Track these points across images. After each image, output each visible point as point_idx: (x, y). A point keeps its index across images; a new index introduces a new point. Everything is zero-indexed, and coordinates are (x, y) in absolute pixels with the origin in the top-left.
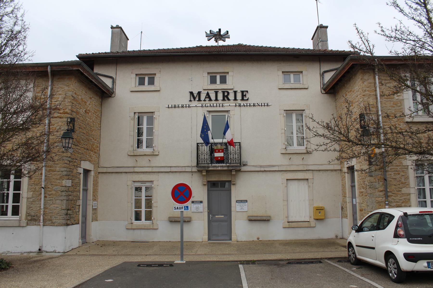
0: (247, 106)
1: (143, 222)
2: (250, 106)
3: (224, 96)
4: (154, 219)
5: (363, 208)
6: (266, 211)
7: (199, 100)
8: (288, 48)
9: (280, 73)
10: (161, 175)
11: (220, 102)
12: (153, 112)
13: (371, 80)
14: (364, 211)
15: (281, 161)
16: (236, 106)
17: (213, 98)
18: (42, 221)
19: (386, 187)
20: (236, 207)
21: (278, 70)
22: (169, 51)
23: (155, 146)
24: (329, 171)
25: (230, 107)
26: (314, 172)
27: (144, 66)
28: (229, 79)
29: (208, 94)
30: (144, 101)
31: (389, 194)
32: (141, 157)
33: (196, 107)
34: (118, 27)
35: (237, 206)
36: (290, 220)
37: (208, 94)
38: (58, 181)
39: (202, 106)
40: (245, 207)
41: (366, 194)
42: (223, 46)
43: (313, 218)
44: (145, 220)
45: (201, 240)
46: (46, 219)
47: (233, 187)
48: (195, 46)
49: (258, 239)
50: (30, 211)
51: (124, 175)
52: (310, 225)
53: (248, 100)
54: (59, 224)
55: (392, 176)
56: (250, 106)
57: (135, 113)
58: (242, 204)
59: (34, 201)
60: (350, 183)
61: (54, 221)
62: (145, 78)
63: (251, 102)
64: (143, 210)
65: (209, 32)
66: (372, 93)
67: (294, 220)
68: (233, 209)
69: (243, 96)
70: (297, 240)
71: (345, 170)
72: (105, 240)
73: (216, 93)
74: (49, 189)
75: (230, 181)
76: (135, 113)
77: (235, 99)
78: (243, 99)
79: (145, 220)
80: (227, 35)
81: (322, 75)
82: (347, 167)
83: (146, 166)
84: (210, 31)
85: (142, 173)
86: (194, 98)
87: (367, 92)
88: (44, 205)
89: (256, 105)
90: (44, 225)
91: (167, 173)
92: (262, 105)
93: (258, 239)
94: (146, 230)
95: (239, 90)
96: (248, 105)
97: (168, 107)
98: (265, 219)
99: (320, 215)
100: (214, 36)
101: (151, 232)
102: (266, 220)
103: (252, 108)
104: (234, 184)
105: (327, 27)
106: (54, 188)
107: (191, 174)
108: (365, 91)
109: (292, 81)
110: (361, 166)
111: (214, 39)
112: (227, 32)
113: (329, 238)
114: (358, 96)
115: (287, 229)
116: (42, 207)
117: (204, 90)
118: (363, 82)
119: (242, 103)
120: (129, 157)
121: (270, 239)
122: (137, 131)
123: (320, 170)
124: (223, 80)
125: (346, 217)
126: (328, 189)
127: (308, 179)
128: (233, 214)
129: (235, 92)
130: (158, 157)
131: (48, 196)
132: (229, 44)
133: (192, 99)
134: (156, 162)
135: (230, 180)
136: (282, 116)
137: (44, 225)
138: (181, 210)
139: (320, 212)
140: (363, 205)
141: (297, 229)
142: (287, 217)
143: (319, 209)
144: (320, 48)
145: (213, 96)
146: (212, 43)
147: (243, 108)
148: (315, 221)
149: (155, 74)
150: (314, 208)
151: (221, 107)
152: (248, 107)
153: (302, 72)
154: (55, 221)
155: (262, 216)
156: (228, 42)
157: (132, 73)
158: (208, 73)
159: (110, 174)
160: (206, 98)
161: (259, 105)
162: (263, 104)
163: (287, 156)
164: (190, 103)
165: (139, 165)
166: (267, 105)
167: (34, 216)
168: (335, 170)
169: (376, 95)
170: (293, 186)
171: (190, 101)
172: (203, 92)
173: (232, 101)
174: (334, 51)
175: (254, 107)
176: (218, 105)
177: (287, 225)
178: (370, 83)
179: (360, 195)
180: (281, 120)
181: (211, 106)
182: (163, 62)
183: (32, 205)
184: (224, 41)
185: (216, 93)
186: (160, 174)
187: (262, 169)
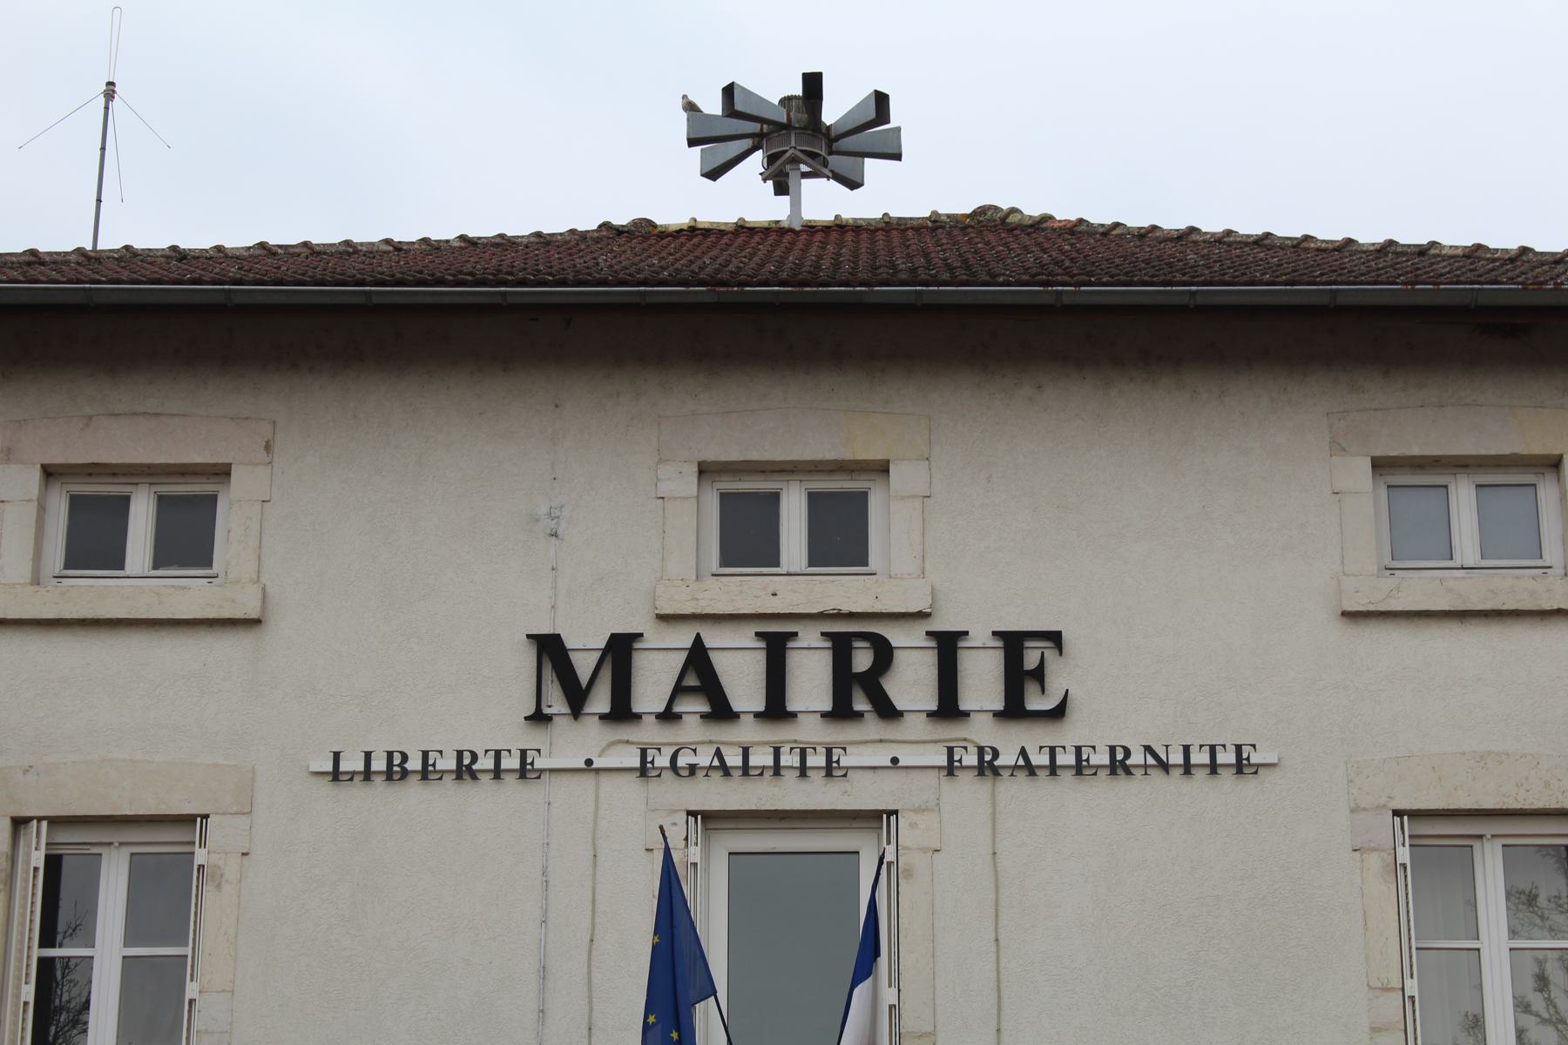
0: (1053, 769)
2: (1079, 768)
3: (843, 680)
7: (622, 712)
8: (1422, 251)
11: (810, 730)
12: (187, 820)
16: (951, 769)
17: (745, 690)
21: (1337, 447)
22: (353, 267)
25: (894, 779)
28: (891, 522)
29: (698, 658)
33: (588, 781)
37: (698, 658)
39: (643, 771)
42: (840, 228)
48: (588, 223)
56: (1079, 768)
57: (19, 823)
62: (125, 501)
63: (1087, 730)
65: (712, 105)
69: (1019, 678)
73: (776, 649)
76: (19, 823)
77: (948, 708)
78: (1013, 710)
80: (874, 131)
84: (729, 91)
86: (577, 698)
89: (1137, 758)
92: (1187, 768)
95: (981, 617)
96: (1066, 759)
97: (336, 775)
100: (758, 141)
103: (1103, 789)
109: (1467, 545)
111: (758, 156)
112: (881, 100)
117: (664, 618)
119: (1010, 742)
122: (29, 992)
124: (841, 537)
129: (948, 646)
132: (895, 213)
133: (556, 703)
136: (1374, 861)
145: (743, 679)
146: (746, 197)
147: (1014, 789)
151: (817, 777)
152: (1067, 777)
156: (887, 193)
158: (705, 471)
160: (679, 690)
161: (1164, 766)
164: (532, 738)
166: (1240, 767)
171: (539, 718)
172: (656, 636)
173: (915, 726)
175: (1122, 784)
176: (789, 759)
180: (1365, 904)
181: (725, 770)
184: (853, 184)
185: (776, 649)
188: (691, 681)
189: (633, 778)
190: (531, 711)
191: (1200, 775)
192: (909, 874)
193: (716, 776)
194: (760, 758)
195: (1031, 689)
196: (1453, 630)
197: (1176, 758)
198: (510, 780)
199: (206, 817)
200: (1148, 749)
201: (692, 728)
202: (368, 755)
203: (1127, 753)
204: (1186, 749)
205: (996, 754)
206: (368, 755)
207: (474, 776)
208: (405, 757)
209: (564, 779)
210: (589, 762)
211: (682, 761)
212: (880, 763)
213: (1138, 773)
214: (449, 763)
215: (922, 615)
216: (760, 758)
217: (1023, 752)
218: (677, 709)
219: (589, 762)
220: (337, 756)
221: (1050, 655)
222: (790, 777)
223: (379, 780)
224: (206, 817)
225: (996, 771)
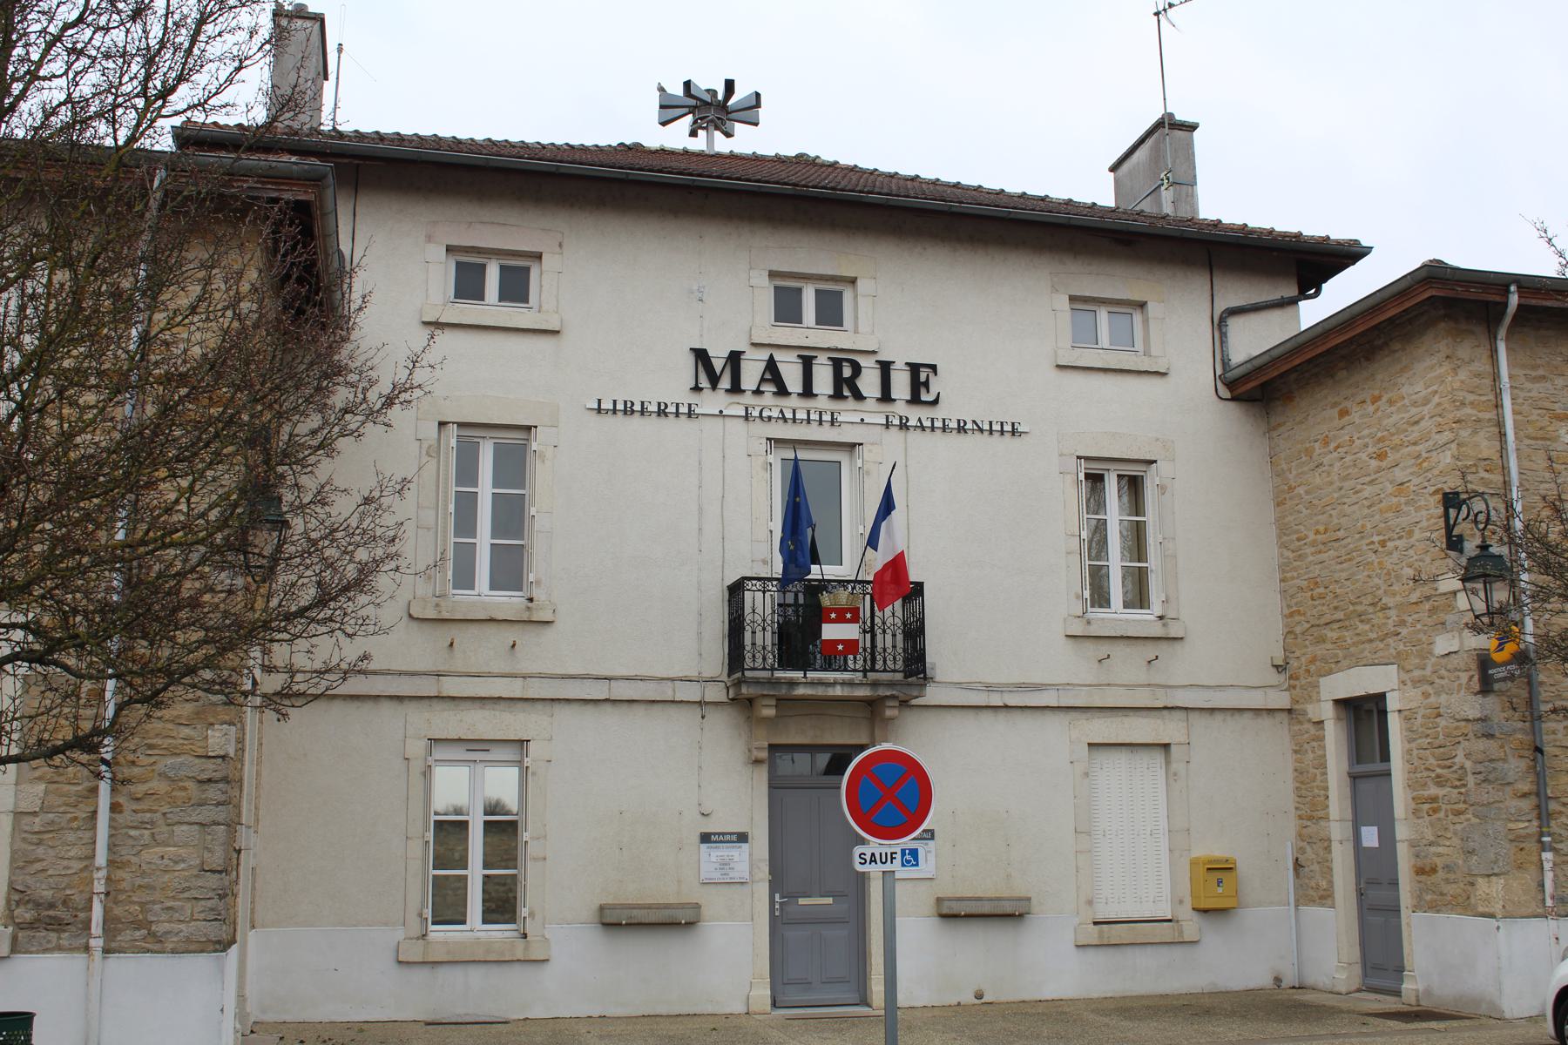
1: (476, 928)
3: (838, 380)
4: (532, 914)
5: (1439, 862)
6: (1009, 876)
7: (736, 388)
9: (1063, 302)
10: (563, 712)
11: (823, 403)
12: (529, 428)
13: (1483, 366)
14: (1441, 874)
15: (1066, 668)
16: (887, 425)
18: (96, 927)
19: (1540, 779)
21: (1055, 290)
23: (538, 582)
26: (1193, 716)
27: (486, 213)
29: (771, 365)
30: (481, 374)
31: (1553, 806)
32: (474, 630)
34: (301, 13)
36: (1100, 917)
37: (771, 365)
38: (186, 731)
39: (746, 417)
41: (1462, 806)
44: (485, 921)
45: (738, 1007)
46: (117, 920)
49: (979, 996)
50: (30, 881)
51: (387, 708)
52: (1181, 932)
53: (936, 402)
54: (188, 940)
55: (1560, 736)
56: (944, 429)
57: (442, 424)
59: (52, 828)
60: (1345, 766)
61: (159, 928)
64: (475, 872)
66: (1488, 416)
67: (1112, 916)
69: (917, 386)
71: (1327, 712)
72: (288, 1018)
73: (807, 363)
74: (136, 771)
76: (442, 424)
77: (886, 397)
78: (915, 400)
79: (485, 921)
80: (750, 110)
81: (1220, 325)
82: (1339, 703)
83: (496, 670)
84: (687, 84)
85: (478, 704)
86: (714, 380)
87: (1468, 410)
88: (112, 847)
90: (107, 951)
91: (590, 708)
93: (979, 996)
94: (495, 969)
95: (900, 358)
96: (938, 424)
98: (1009, 910)
99: (1216, 893)
100: (692, 110)
101: (515, 977)
102: (1007, 915)
105: (1192, 127)
106: (160, 767)
107: (697, 711)
108: (1463, 404)
109: (1104, 341)
110: (1426, 695)
111: (690, 118)
112: (758, 95)
113: (1251, 986)
114: (1423, 424)
115: (1091, 953)
116: (101, 858)
117: (753, 344)
118: (1455, 370)
119: (914, 415)
120: (414, 625)
121: (1027, 997)
123: (1212, 710)
124: (830, 313)
125: (1325, 897)
126: (1242, 791)
127: (1166, 746)
129: (885, 368)
130: (549, 634)
131: (128, 806)
133: (704, 382)
134: (545, 654)
136: (1070, 479)
137: (107, 951)
138: (888, 867)
139: (1219, 882)
140: (1440, 850)
141: (1129, 951)
142: (1090, 903)
143: (1221, 869)
144: (1168, 209)
145: (792, 375)
146: (678, 137)
147: (915, 436)
148: (1195, 916)
149: (538, 257)
150: (1194, 863)
151: (826, 426)
152: (938, 432)
153: (1142, 305)
154: (167, 926)
155: (999, 899)
156: (744, 141)
157: (429, 239)
160: (763, 380)
161: (981, 430)
162: (996, 427)
163: (1089, 644)
164: (693, 398)
167: (52, 906)
168: (1270, 711)
169: (1500, 424)
170: (1115, 772)
171: (697, 389)
172: (751, 353)
173: (871, 404)
174: (1253, 231)
176: (815, 416)
177: (1092, 934)
178: (1478, 375)
179: (1416, 812)
180: (1069, 495)
181: (785, 420)
182: (572, 206)
183: (40, 851)
184: (728, 135)
185: (807, 363)
186: (557, 706)
187: (996, 700)
191: (996, 435)
192: (868, 473)
194: (801, 415)
195: (923, 391)
196: (1101, 377)
197: (986, 427)
198: (683, 418)
201: (768, 399)
207: (666, 415)
214: (654, 408)
215: (874, 352)
216: (801, 415)
222: (814, 425)
223: (620, 414)
225: (907, 428)
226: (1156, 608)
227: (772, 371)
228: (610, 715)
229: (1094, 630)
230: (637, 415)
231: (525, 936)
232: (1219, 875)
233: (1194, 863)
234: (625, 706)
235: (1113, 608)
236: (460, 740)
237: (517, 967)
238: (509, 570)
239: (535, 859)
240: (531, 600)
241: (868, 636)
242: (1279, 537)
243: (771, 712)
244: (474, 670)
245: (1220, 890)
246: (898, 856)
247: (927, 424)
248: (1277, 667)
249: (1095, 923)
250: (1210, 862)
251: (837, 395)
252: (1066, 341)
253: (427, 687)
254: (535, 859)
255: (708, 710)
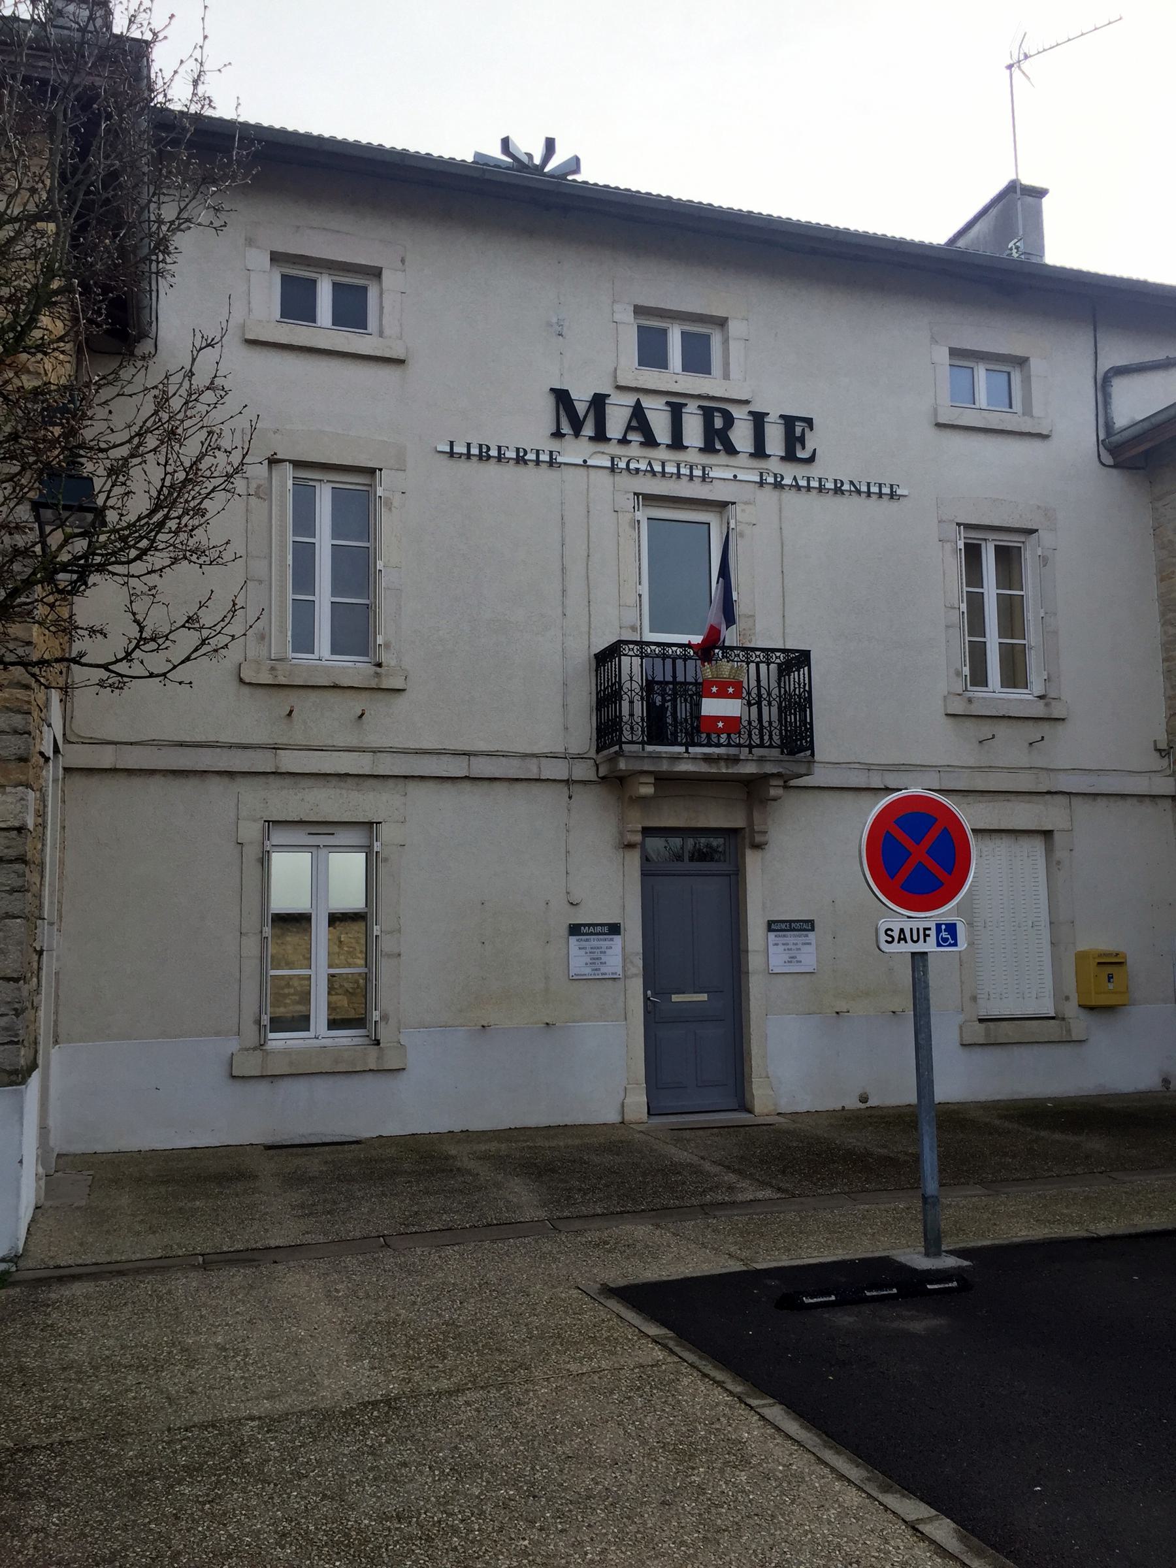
2: (821, 489)
7: (600, 436)
9: (942, 355)
10: (416, 791)
12: (371, 472)
16: (761, 484)
17: (662, 433)
20: (766, 954)
23: (387, 645)
24: (1130, 801)
25: (733, 486)
26: (1074, 800)
29: (638, 412)
32: (313, 696)
33: (583, 471)
35: (772, 949)
36: (983, 1013)
37: (638, 412)
39: (613, 469)
40: (809, 952)
43: (1074, 1002)
45: (613, 1117)
47: (753, 862)
49: (864, 1099)
51: (215, 786)
52: (1069, 1031)
53: (811, 459)
58: (791, 938)
62: (314, 282)
63: (825, 470)
68: (754, 962)
69: (793, 441)
70: (1049, 1099)
73: (676, 411)
75: (734, 831)
77: (759, 452)
78: (790, 457)
81: (1103, 386)
83: (340, 742)
89: (846, 487)
91: (448, 786)
93: (864, 1099)
95: (775, 406)
97: (451, 454)
103: (830, 501)
104: (758, 847)
115: (978, 1055)
119: (790, 472)
120: (246, 690)
123: (1095, 795)
127: (1047, 834)
128: (756, 986)
129: (759, 419)
130: (401, 702)
133: (566, 429)
135: (738, 822)
136: (948, 546)
139: (1110, 978)
142: (974, 999)
147: (789, 496)
148: (1083, 1014)
149: (376, 273)
152: (814, 492)
158: (639, 311)
159: (137, 782)
160: (629, 428)
161: (859, 492)
162: (875, 489)
163: (969, 724)
164: (555, 445)
165: (300, 739)
168: (1153, 797)
171: (558, 434)
173: (742, 460)
175: (839, 499)
177: (978, 1032)
181: (653, 473)
185: (676, 411)
186: (411, 786)
188: (634, 423)
189: (607, 471)
190: (554, 431)
191: (874, 497)
193: (649, 475)
195: (798, 447)
197: (864, 489)
199: (381, 470)
200: (851, 483)
201: (634, 450)
202: (469, 445)
203: (842, 484)
204: (869, 484)
205: (782, 478)
206: (469, 445)
208: (488, 448)
209: (572, 469)
210: (585, 461)
211: (632, 466)
212: (729, 476)
213: (847, 494)
214: (511, 454)
215: (747, 402)
217: (795, 478)
218: (629, 438)
219: (585, 461)
220: (452, 444)
221: (807, 430)
222: (685, 479)
223: (474, 459)
224: (381, 470)
226: (1037, 687)
227: (639, 420)
228: (471, 797)
229: (975, 709)
230: (493, 461)
231: (377, 1042)
232: (1110, 969)
233: (1081, 957)
234: (486, 783)
235: (990, 688)
236: (301, 822)
237: (369, 1077)
238: (355, 631)
239: (389, 956)
240: (379, 665)
241: (754, 709)
242: (1163, 614)
243: (647, 790)
244: (315, 743)
245: (1111, 986)
246: (933, 933)
247: (803, 483)
248: (1160, 751)
249: (981, 1021)
250: (1100, 955)
251: (708, 448)
252: (945, 399)
253: (262, 761)
254: (389, 956)
255: (575, 789)
